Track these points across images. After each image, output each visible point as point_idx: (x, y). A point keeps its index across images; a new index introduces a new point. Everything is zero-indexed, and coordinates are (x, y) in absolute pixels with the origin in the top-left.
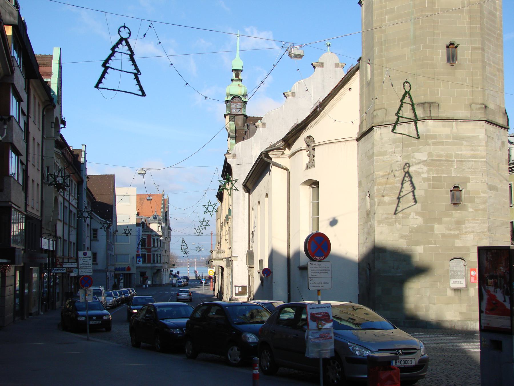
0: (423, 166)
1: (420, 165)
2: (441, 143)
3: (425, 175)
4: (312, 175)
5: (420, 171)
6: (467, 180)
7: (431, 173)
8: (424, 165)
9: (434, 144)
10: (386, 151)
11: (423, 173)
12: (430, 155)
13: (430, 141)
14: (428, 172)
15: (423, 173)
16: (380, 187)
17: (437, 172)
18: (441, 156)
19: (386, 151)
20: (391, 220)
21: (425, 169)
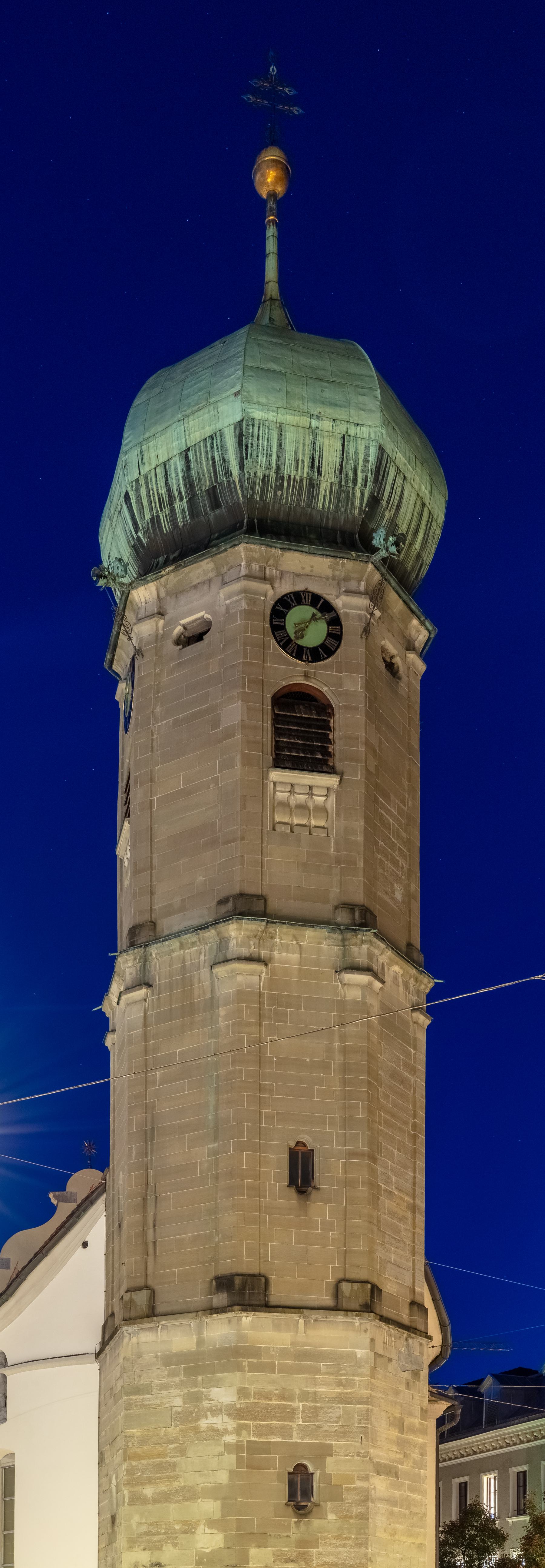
0: (226, 1418)
1: (220, 1417)
3: (232, 1439)
5: (221, 1427)
7: (244, 1433)
8: (229, 1415)
9: (253, 1368)
10: (149, 1385)
11: (226, 1432)
12: (242, 1393)
13: (245, 1363)
14: (238, 1431)
15: (226, 1432)
16: (134, 1463)
20: (156, 1538)
21: (231, 1425)
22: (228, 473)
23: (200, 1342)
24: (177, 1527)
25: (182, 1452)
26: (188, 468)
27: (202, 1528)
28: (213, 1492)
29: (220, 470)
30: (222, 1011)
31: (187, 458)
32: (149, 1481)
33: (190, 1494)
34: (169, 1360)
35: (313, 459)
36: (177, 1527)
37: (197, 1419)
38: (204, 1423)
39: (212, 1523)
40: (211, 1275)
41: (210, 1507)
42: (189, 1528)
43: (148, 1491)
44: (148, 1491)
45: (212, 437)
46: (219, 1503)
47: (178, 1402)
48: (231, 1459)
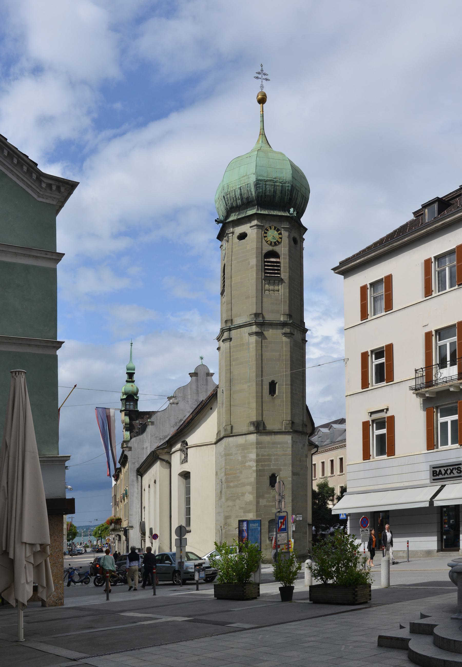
0: (253, 463)
2: (265, 448)
4: (186, 467)
5: (252, 465)
6: (280, 470)
10: (232, 453)
11: (253, 467)
17: (262, 466)
18: (264, 455)
19: (232, 453)
20: (234, 498)
22: (252, 194)
23: (246, 441)
24: (240, 494)
25: (241, 473)
26: (241, 192)
27: (247, 495)
28: (249, 484)
29: (249, 193)
30: (251, 346)
31: (241, 189)
32: (232, 481)
33: (243, 485)
34: (237, 446)
35: (274, 190)
36: (240, 494)
37: (245, 463)
38: (247, 464)
39: (250, 493)
40: (248, 422)
41: (249, 488)
42: (243, 494)
43: (232, 484)
44: (232, 484)
45: (247, 184)
46: (251, 487)
47: (240, 458)
48: (255, 474)
